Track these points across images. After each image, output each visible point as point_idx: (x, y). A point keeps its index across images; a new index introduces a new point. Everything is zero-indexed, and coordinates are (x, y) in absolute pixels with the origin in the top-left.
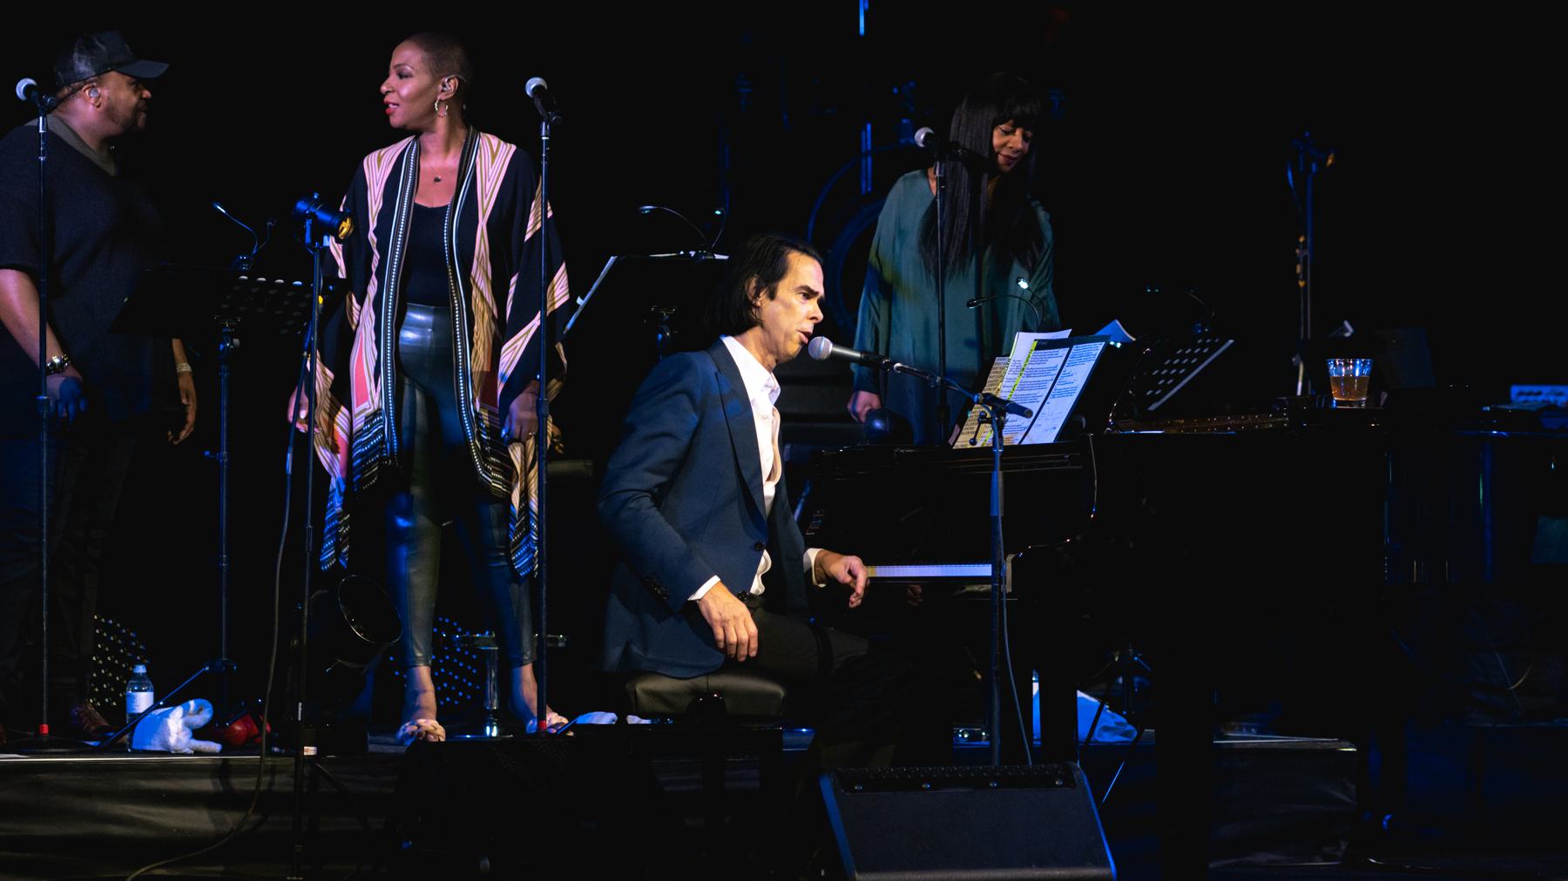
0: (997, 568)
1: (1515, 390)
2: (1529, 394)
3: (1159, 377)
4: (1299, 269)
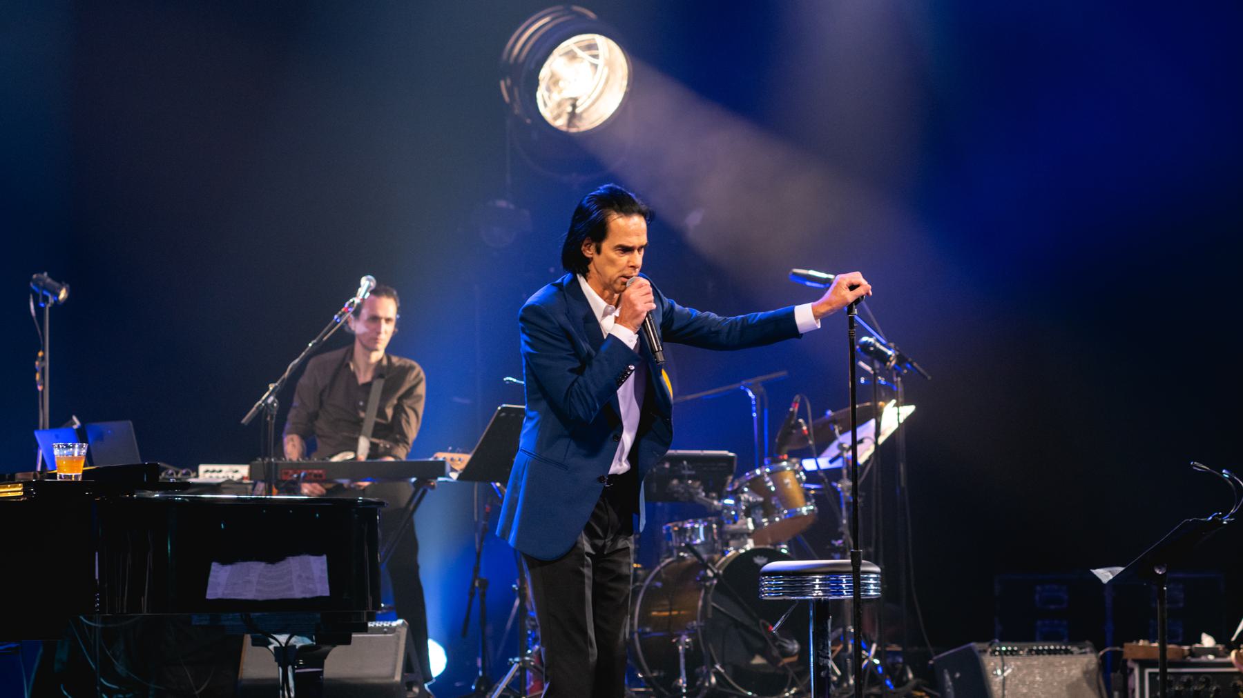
1: (202, 468)
2: (214, 471)
4: (38, 376)
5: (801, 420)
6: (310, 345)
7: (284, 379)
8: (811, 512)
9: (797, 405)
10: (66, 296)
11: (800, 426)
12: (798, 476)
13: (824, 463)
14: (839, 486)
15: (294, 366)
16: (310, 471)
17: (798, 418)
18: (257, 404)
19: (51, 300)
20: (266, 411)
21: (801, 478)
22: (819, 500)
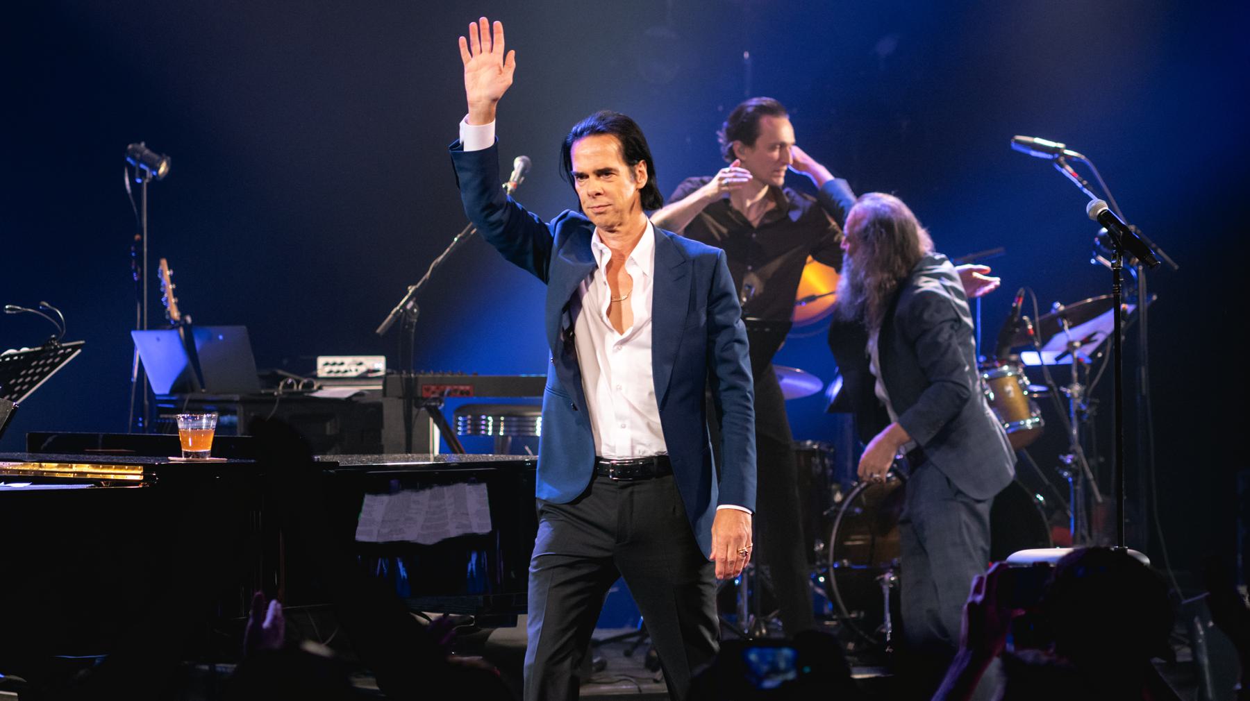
1: (321, 360)
2: (334, 364)
3: (16, 384)
5: (1025, 318)
6: (456, 239)
7: (426, 280)
8: (1037, 426)
9: (1021, 300)
10: (167, 170)
11: (1024, 324)
12: (1021, 382)
13: (1048, 358)
14: (1069, 391)
15: (436, 263)
16: (455, 387)
17: (1023, 314)
18: (395, 310)
19: (149, 174)
20: (405, 319)
21: (1024, 383)
22: (1042, 404)
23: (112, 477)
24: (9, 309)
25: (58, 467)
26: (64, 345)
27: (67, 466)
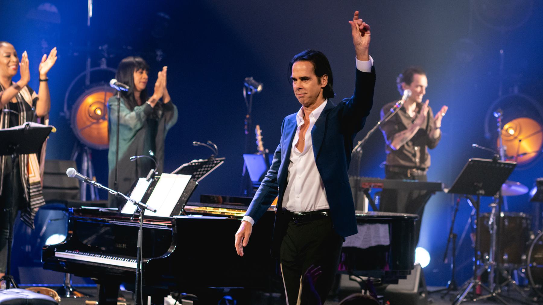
0: (139, 266)
3: (196, 175)
10: (261, 90)
19: (254, 90)
23: (235, 215)
24: (195, 144)
25: (214, 209)
26: (217, 159)
27: (217, 209)
